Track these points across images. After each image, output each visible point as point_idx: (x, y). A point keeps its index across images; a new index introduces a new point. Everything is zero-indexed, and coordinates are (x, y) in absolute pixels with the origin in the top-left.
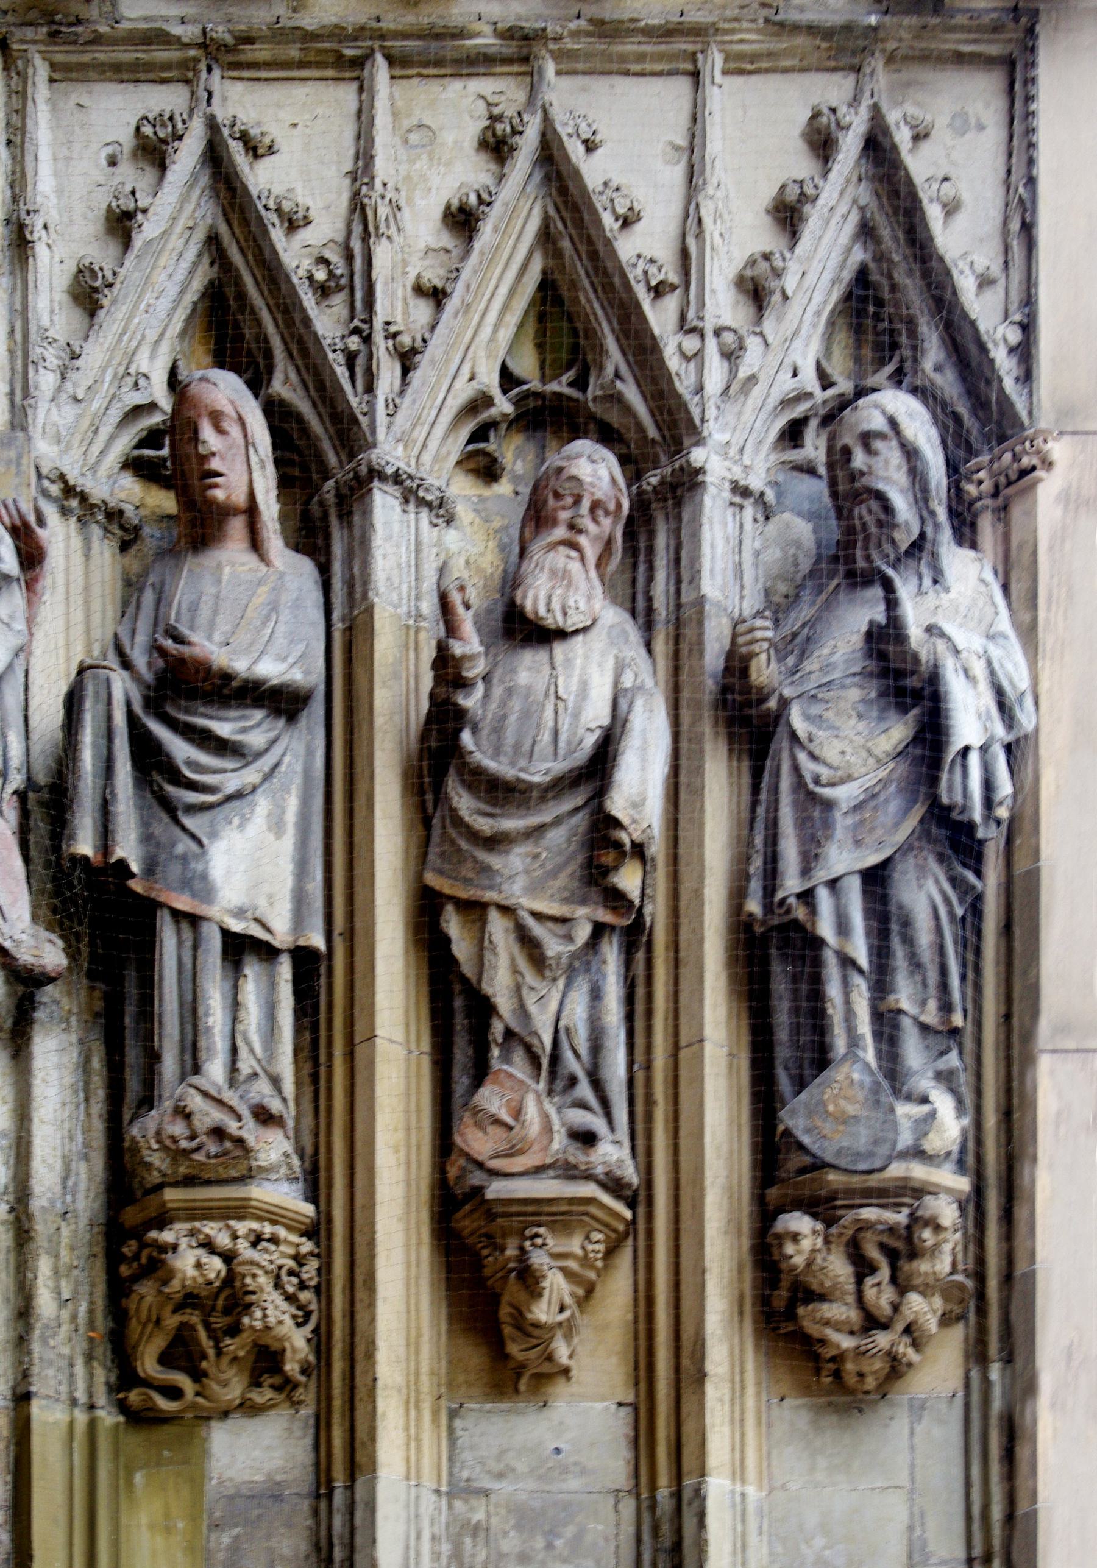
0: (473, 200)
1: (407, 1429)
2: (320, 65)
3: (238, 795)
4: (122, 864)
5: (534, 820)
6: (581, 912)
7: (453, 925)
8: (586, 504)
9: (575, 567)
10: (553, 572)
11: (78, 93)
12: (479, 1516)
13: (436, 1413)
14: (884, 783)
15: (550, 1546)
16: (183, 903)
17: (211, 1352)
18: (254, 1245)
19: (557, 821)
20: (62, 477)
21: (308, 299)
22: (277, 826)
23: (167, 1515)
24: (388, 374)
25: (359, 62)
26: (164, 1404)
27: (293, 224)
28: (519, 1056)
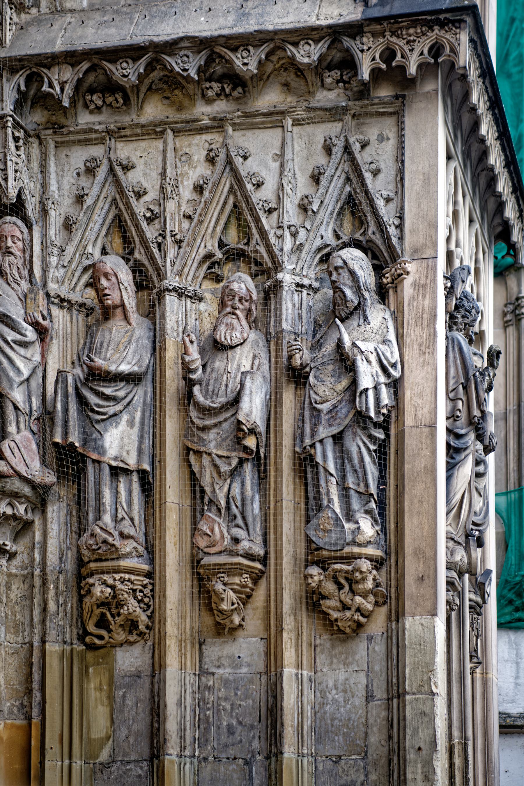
0: (201, 182)
1: (180, 650)
2: (149, 134)
3: (115, 415)
4: (72, 444)
5: (217, 420)
6: (234, 454)
7: (192, 459)
8: (237, 299)
9: (235, 322)
10: (227, 324)
12: (211, 683)
13: (193, 644)
14: (340, 402)
15: (236, 694)
16: (95, 456)
17: (113, 622)
18: (122, 582)
19: (226, 420)
20: (59, 296)
21: (144, 224)
22: (131, 424)
23: (101, 684)
24: (172, 252)
25: (163, 132)
26: (97, 641)
27: (139, 195)
28: (214, 508)
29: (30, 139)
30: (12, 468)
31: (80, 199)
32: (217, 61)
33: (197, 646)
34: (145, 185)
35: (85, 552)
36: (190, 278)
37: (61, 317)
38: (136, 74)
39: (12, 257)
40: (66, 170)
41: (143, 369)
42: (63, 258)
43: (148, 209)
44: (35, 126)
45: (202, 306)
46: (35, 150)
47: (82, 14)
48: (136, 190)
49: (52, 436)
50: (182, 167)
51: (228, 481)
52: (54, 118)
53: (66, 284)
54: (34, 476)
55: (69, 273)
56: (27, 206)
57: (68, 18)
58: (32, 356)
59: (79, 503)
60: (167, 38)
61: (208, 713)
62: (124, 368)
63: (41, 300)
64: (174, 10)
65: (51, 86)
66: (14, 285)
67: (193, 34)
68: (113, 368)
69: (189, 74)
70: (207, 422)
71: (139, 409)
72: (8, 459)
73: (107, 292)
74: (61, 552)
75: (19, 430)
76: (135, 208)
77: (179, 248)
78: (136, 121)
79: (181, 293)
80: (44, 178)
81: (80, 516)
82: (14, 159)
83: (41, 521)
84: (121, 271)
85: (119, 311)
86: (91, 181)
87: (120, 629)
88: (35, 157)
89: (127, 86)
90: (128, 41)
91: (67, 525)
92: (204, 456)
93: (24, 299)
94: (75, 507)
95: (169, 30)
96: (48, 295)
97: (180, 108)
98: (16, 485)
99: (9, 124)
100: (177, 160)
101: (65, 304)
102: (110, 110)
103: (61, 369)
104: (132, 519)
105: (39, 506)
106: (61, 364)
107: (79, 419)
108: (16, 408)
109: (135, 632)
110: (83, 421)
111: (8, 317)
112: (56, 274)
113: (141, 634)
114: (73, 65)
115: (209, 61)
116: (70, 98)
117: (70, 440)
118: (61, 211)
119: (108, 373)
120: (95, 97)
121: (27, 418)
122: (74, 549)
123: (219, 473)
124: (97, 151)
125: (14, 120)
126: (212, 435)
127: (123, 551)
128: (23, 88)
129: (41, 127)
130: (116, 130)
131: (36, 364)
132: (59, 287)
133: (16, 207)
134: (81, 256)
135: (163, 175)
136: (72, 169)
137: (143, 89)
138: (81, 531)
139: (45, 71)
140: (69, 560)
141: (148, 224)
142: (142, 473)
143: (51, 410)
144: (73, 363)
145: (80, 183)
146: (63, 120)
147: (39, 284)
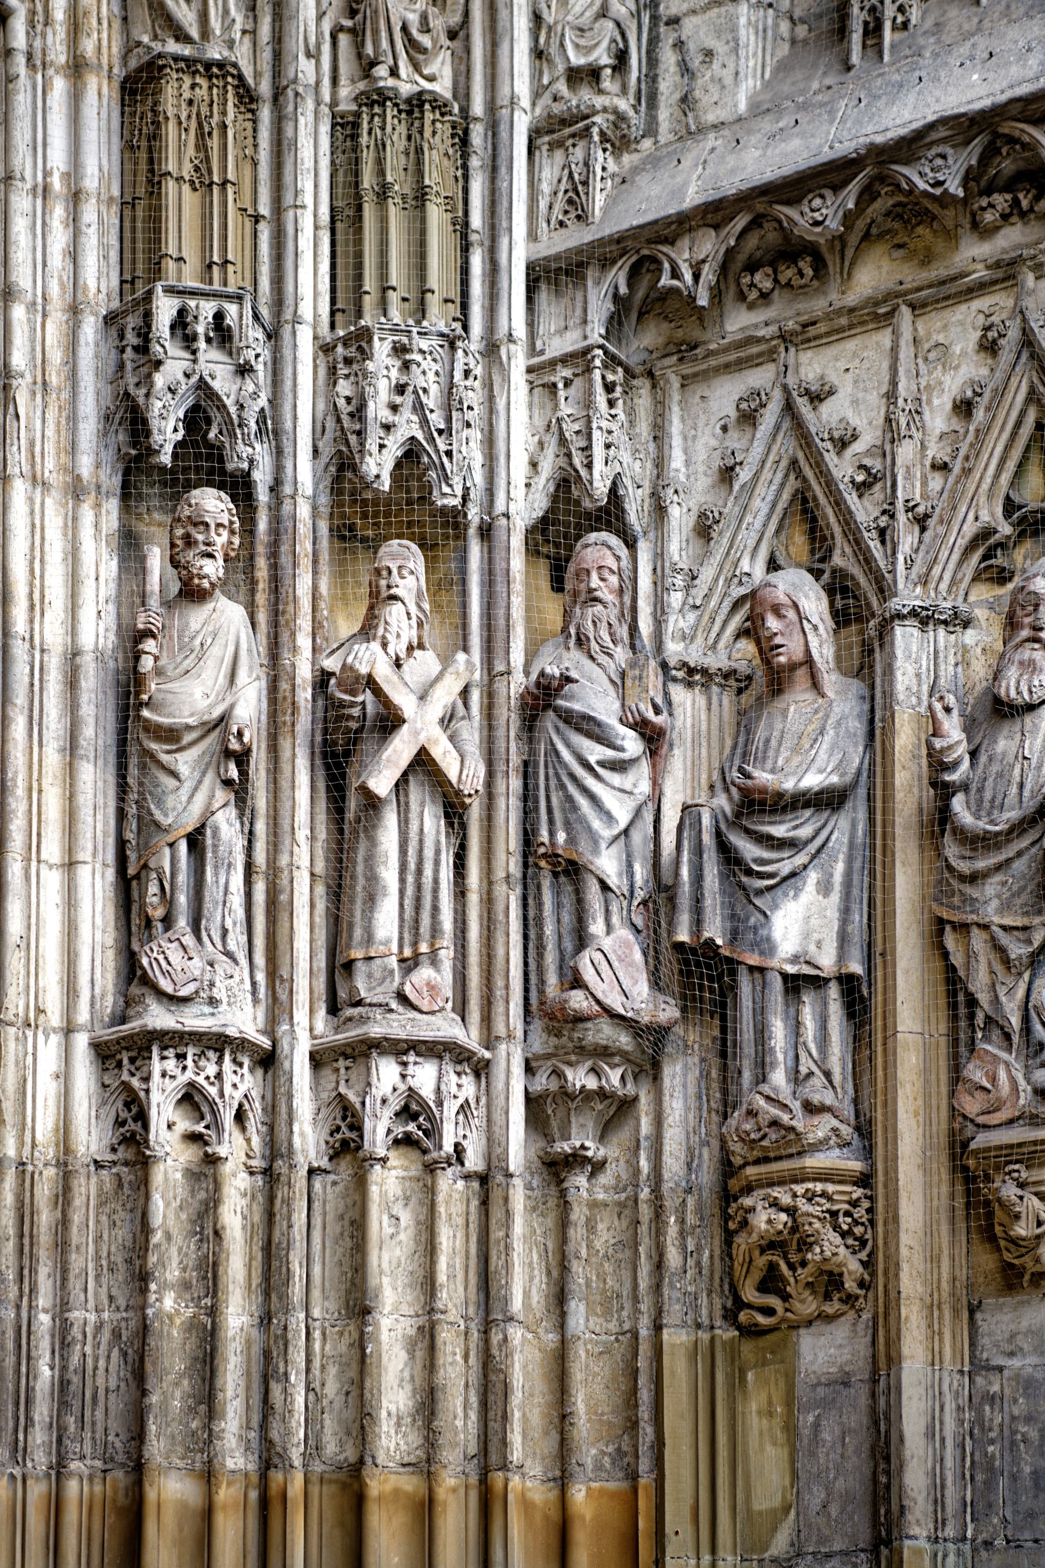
0: (969, 393)
2: (862, 323)
3: (793, 875)
4: (710, 943)
5: (1001, 857)
11: (700, 389)
19: (1019, 854)
21: (852, 499)
24: (907, 540)
25: (891, 314)
27: (842, 444)
29: (635, 382)
30: (598, 1002)
31: (727, 474)
32: (1004, 151)
33: (965, 1315)
34: (855, 421)
35: (737, 1147)
36: (943, 586)
37: (689, 703)
38: (841, 213)
39: (600, 607)
40: (701, 424)
41: (848, 778)
42: (693, 592)
43: (862, 467)
44: (644, 355)
45: (970, 637)
46: (644, 400)
47: (736, 127)
48: (836, 435)
49: (670, 933)
50: (930, 373)
51: (1026, 976)
52: (680, 334)
53: (699, 640)
54: (637, 1012)
55: (706, 618)
56: (627, 506)
57: (711, 140)
58: (635, 785)
59: (723, 1055)
60: (902, 132)
61: (991, 1449)
62: (812, 781)
63: (652, 677)
64: (917, 74)
65: (675, 274)
66: (602, 658)
67: (956, 111)
68: (788, 785)
69: (946, 190)
70: (981, 864)
71: (841, 856)
72: (590, 985)
73: (778, 640)
74: (690, 1151)
75: (609, 929)
76: (834, 471)
77: (923, 529)
78: (837, 305)
79: (924, 618)
80: (660, 449)
81: (725, 1078)
82: (604, 424)
83: (651, 1096)
84: (806, 597)
85: (801, 673)
86: (748, 436)
87: (807, 1293)
89: (822, 241)
90: (827, 155)
91: (700, 1098)
92: (975, 931)
93: (621, 682)
94: (716, 1061)
95: (907, 115)
96: (664, 666)
97: (927, 259)
98: (605, 1033)
99: (598, 362)
100: (920, 361)
101: (697, 677)
102: (787, 294)
103: (690, 802)
104: (828, 1075)
105: (648, 1067)
106: (689, 792)
107: (723, 892)
108: (605, 887)
109: (836, 1296)
110: (731, 895)
111: (591, 719)
112: (681, 624)
113: (849, 1299)
114: (716, 227)
115: (988, 154)
116: (711, 289)
117: (706, 935)
118: (691, 504)
119: (780, 795)
120: (758, 277)
121: (625, 903)
122: (715, 1144)
123: (1006, 962)
124: (761, 377)
126: (991, 888)
127: (811, 1138)
128: (623, 290)
129: (655, 355)
130: (798, 328)
131: (641, 798)
132: (686, 648)
133: (608, 512)
134: (728, 582)
135: (891, 396)
136: (713, 421)
137: (853, 240)
138: (727, 1107)
139: (665, 249)
140: (705, 1166)
141: (860, 496)
142: (848, 983)
143: (670, 883)
144: (712, 787)
145: (727, 444)
146: (697, 334)
147: (648, 648)
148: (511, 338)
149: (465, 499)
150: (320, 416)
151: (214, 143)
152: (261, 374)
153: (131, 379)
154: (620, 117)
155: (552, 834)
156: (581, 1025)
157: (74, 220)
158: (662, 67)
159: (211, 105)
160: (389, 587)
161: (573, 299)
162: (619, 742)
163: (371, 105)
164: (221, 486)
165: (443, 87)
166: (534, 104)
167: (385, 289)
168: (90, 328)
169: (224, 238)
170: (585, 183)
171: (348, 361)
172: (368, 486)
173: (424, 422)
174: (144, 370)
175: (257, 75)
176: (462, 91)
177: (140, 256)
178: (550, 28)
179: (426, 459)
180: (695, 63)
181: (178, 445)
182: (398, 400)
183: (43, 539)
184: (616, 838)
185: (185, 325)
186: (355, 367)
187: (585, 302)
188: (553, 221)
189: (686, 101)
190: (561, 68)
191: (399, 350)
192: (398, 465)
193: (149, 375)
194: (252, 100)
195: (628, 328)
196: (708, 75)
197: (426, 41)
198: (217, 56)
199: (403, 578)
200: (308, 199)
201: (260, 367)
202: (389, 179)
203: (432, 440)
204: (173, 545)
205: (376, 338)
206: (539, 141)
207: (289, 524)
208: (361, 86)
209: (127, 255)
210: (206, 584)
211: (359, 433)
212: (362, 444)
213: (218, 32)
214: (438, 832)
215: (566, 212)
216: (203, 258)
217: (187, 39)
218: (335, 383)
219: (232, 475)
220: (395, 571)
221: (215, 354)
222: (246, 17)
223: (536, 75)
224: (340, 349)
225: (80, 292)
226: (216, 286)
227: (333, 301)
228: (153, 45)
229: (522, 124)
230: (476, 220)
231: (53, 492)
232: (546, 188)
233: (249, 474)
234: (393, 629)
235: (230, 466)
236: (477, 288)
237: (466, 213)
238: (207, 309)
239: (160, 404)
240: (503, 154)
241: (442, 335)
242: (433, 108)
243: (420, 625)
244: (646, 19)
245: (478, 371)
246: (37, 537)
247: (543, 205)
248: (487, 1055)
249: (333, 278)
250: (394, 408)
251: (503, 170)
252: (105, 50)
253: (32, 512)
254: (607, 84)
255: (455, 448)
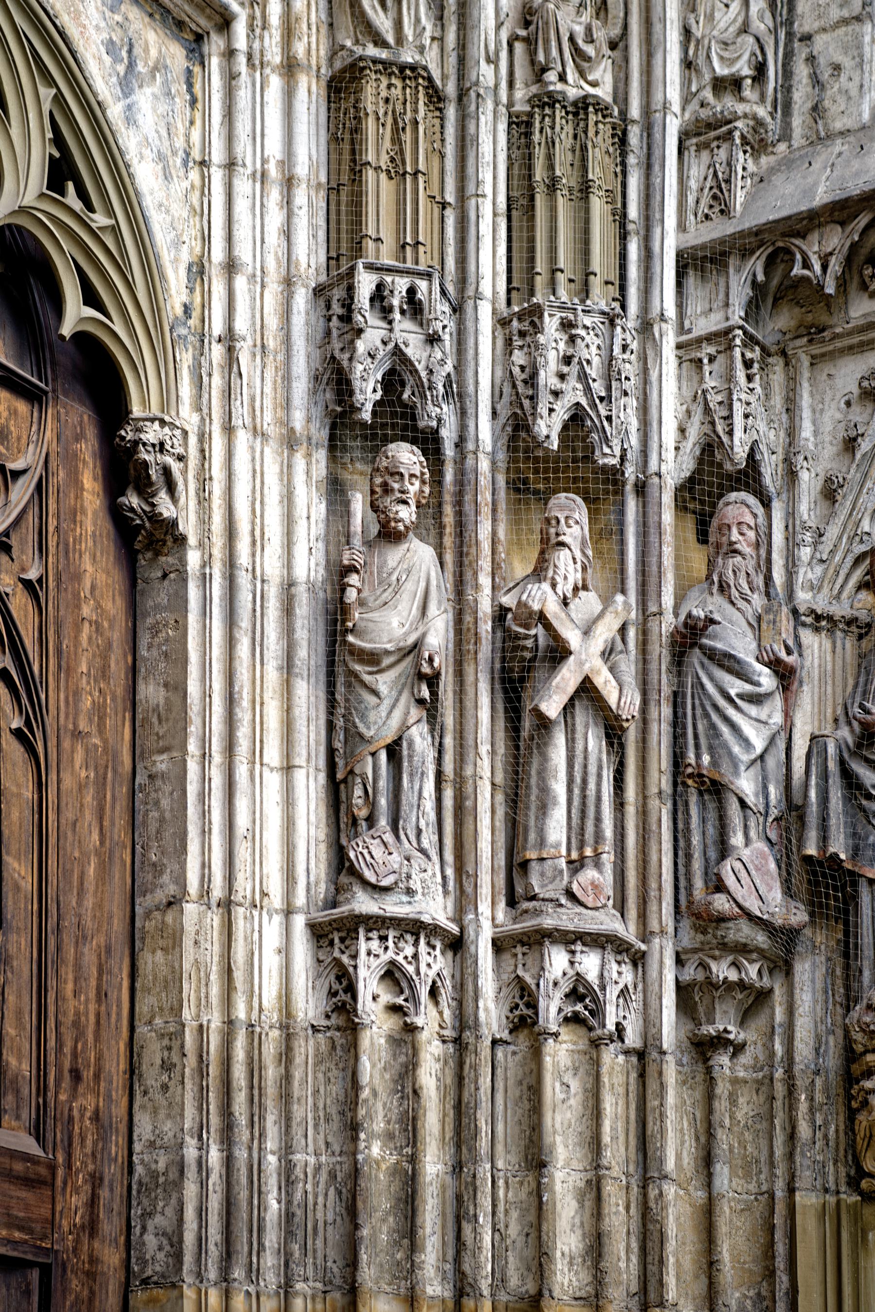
11: (828, 368)
29: (770, 360)
31: (850, 444)
35: (858, 1037)
37: (816, 646)
40: (827, 399)
42: (820, 547)
44: (779, 336)
46: (778, 376)
47: (861, 134)
49: (800, 847)
52: (810, 318)
53: (826, 590)
54: (773, 915)
55: (831, 571)
56: (763, 470)
57: (838, 146)
58: (769, 716)
59: (846, 955)
63: (784, 622)
65: (806, 265)
66: (741, 604)
72: (732, 890)
74: (818, 1038)
75: (748, 842)
80: (792, 420)
81: (848, 976)
82: (743, 396)
83: (784, 989)
88: (777, 388)
91: (826, 992)
93: (757, 625)
94: (839, 961)
96: (795, 612)
98: (744, 932)
99: (738, 341)
101: (824, 623)
103: (817, 733)
105: (781, 963)
106: (816, 723)
107: (846, 813)
108: (743, 804)
110: (853, 816)
111: (731, 657)
112: (810, 575)
114: (843, 224)
116: (837, 278)
117: (832, 850)
118: (819, 470)
121: (761, 819)
122: (840, 1032)
125: (745, 333)
128: (760, 277)
129: (788, 337)
131: (775, 728)
132: (814, 597)
133: (746, 475)
134: (851, 540)
136: (838, 397)
138: (850, 1001)
139: (797, 242)
140: (831, 1051)
143: (800, 803)
144: (836, 720)
145: (850, 417)
146: (824, 319)
147: (781, 596)
148: (662, 318)
149: (623, 458)
150: (498, 381)
151: (407, 137)
152: (447, 343)
153: (337, 345)
154: (759, 123)
155: (698, 756)
156: (723, 925)
157: (288, 202)
158: (796, 78)
159: (404, 103)
160: (558, 535)
161: (717, 285)
162: (756, 678)
163: (542, 107)
164: (413, 441)
165: (604, 92)
166: (683, 109)
167: (554, 271)
168: (301, 299)
169: (416, 222)
170: (728, 181)
171: (522, 334)
172: (539, 445)
173: (588, 390)
174: (348, 337)
175: (444, 77)
176: (621, 96)
177: (344, 235)
178: (698, 42)
179: (589, 423)
180: (825, 75)
181: (377, 404)
182: (565, 369)
183: (262, 483)
184: (753, 762)
185: (382, 298)
186: (528, 339)
187: (728, 287)
188: (700, 214)
189: (817, 110)
190: (707, 77)
191: (567, 325)
192: (565, 427)
193: (352, 342)
194: (440, 99)
195: (765, 312)
196: (837, 86)
197: (590, 50)
198: (410, 60)
199: (569, 527)
200: (488, 189)
201: (446, 337)
202: (558, 173)
203: (594, 406)
204: (373, 492)
205: (546, 314)
206: (688, 143)
207: (472, 477)
208: (534, 89)
209: (333, 235)
210: (401, 527)
211: (531, 398)
212: (534, 408)
213: (411, 39)
214: (600, 751)
215: (711, 207)
216: (398, 239)
217: (384, 44)
218: (511, 353)
219: (423, 432)
220: (563, 521)
221: (408, 325)
222: (435, 25)
223: (686, 83)
224: (515, 323)
225: (293, 266)
226: (409, 265)
227: (509, 280)
228: (355, 48)
229: (673, 127)
230: (633, 212)
231: (271, 442)
232: (693, 184)
233: (437, 431)
234: (561, 571)
235: (421, 424)
236: (633, 272)
237: (624, 205)
238: (402, 284)
239: (360, 367)
240: (657, 153)
241: (603, 313)
242: (596, 111)
243: (584, 569)
244: (782, 36)
245: (634, 346)
246: (258, 481)
247: (691, 199)
248: (643, 947)
249: (509, 260)
250: (562, 377)
251: (656, 168)
252: (314, 53)
253: (253, 459)
254: (747, 93)
255: (614, 413)
